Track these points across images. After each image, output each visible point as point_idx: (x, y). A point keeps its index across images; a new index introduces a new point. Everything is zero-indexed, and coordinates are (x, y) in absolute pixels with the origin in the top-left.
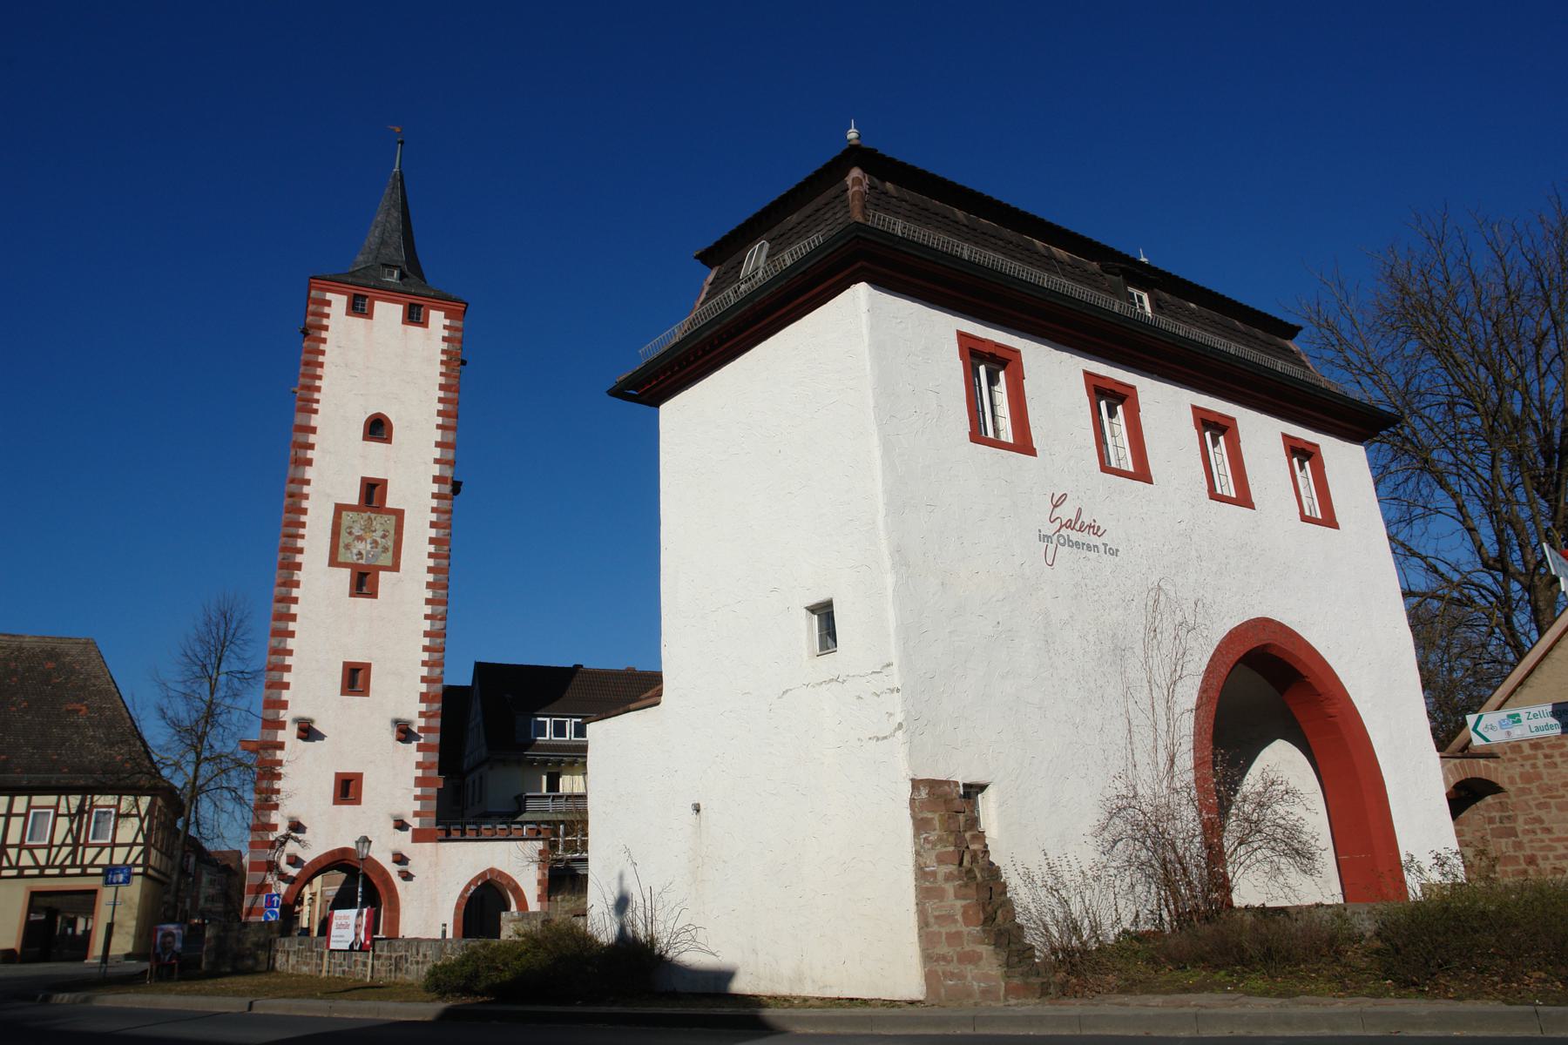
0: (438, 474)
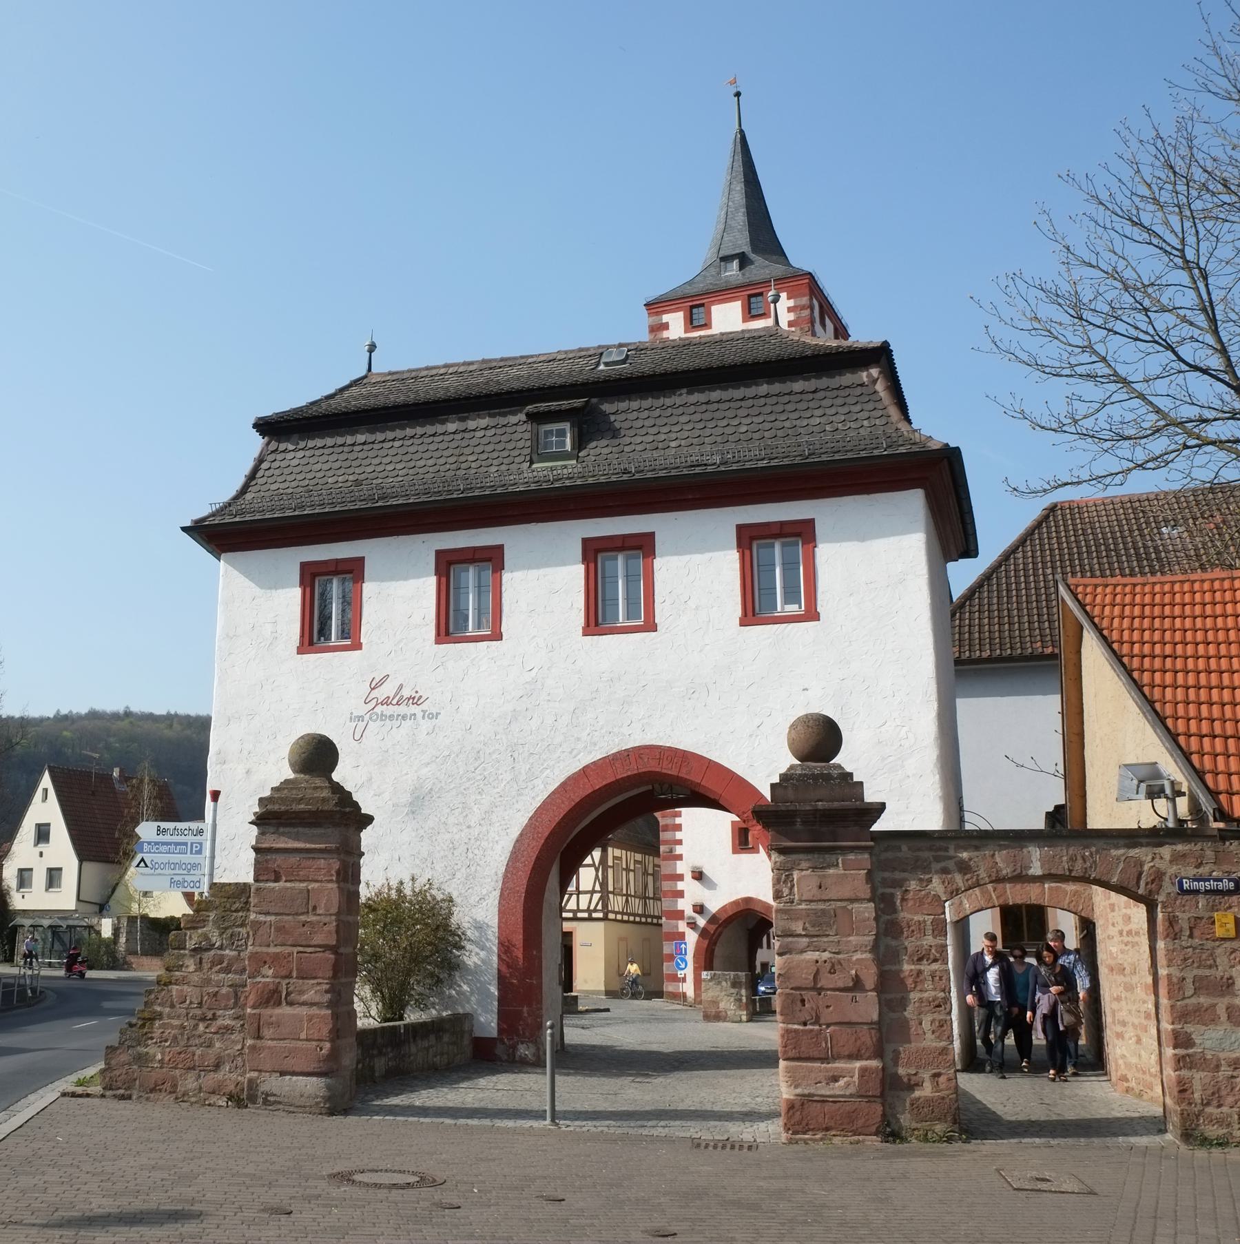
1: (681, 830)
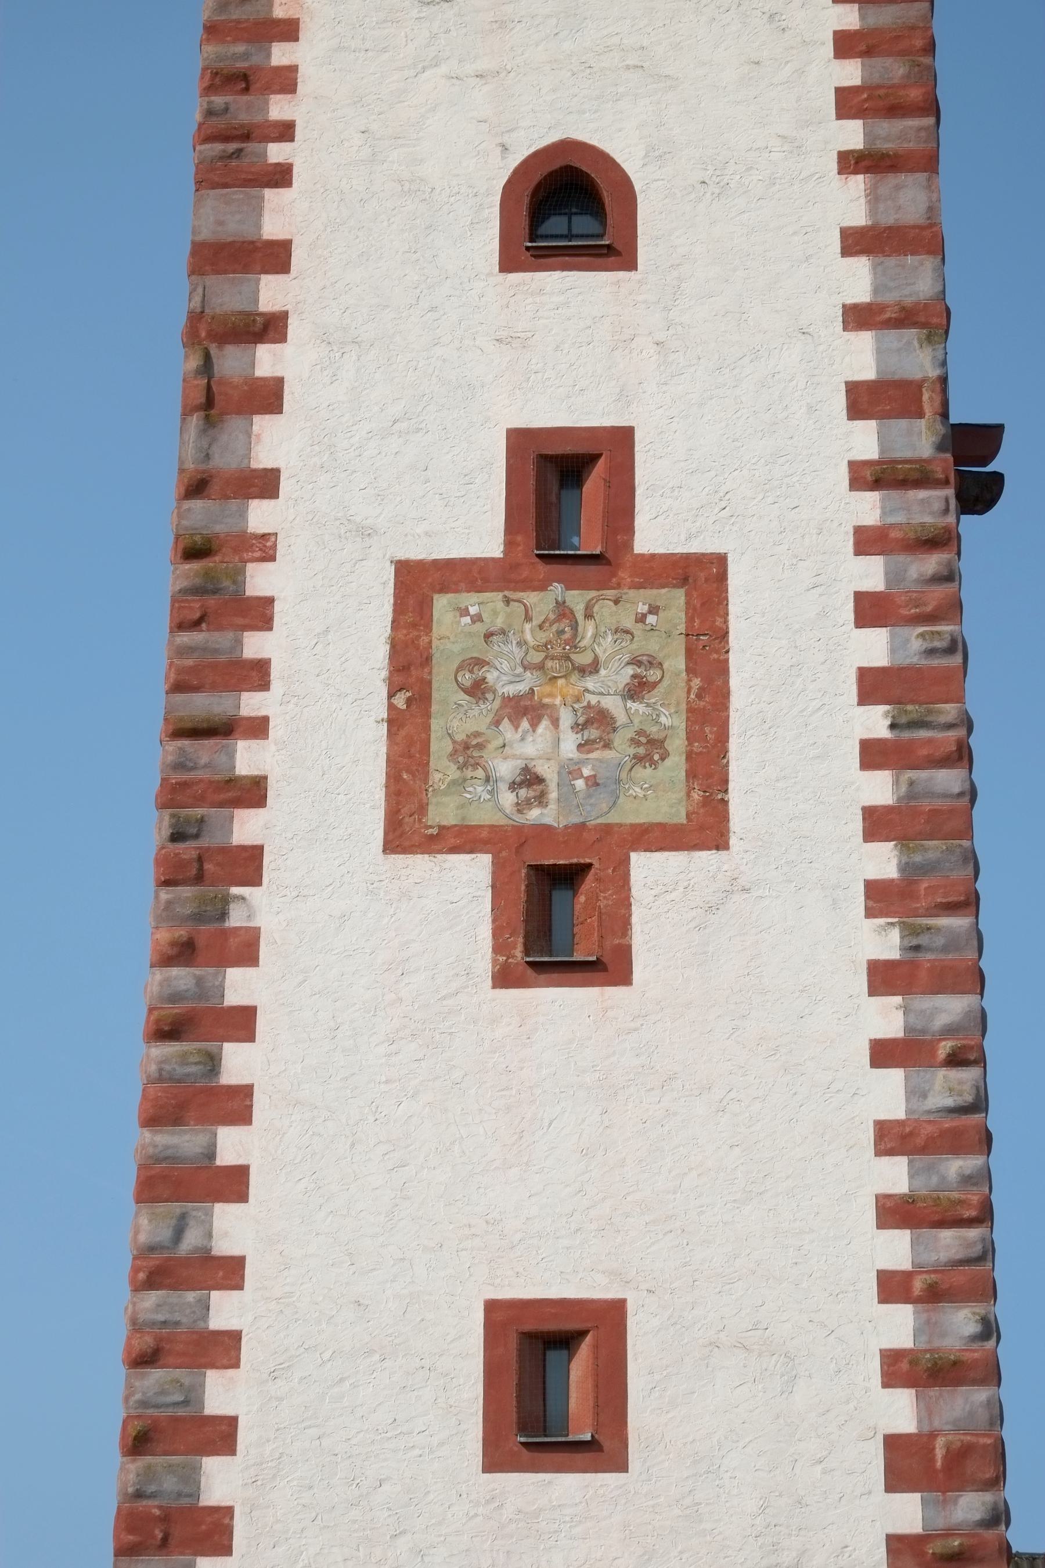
0: (869, 374)
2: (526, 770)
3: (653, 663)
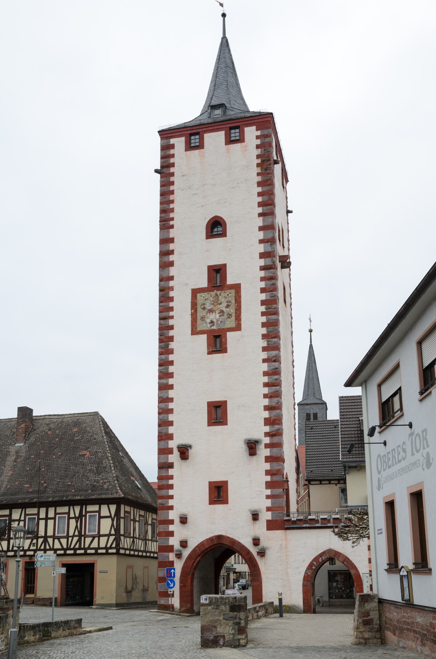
0: (263, 251)
1: (173, 489)
2: (211, 321)
3: (230, 302)
